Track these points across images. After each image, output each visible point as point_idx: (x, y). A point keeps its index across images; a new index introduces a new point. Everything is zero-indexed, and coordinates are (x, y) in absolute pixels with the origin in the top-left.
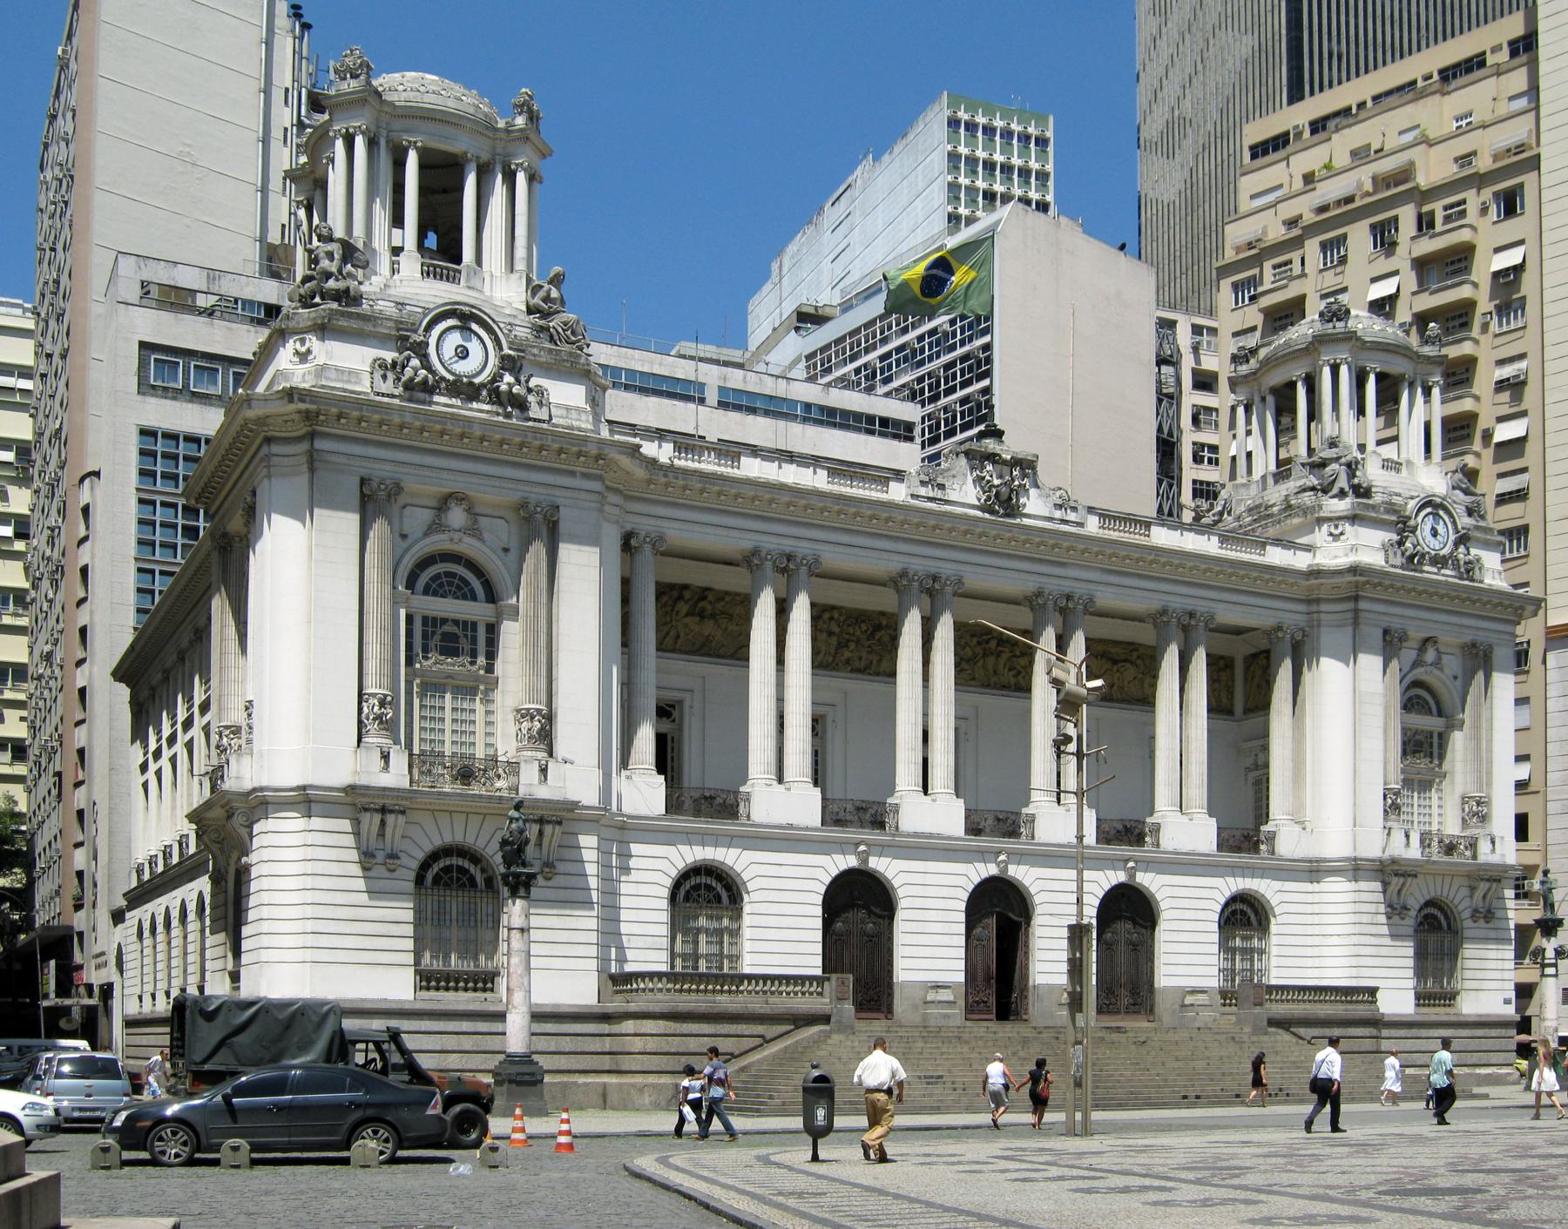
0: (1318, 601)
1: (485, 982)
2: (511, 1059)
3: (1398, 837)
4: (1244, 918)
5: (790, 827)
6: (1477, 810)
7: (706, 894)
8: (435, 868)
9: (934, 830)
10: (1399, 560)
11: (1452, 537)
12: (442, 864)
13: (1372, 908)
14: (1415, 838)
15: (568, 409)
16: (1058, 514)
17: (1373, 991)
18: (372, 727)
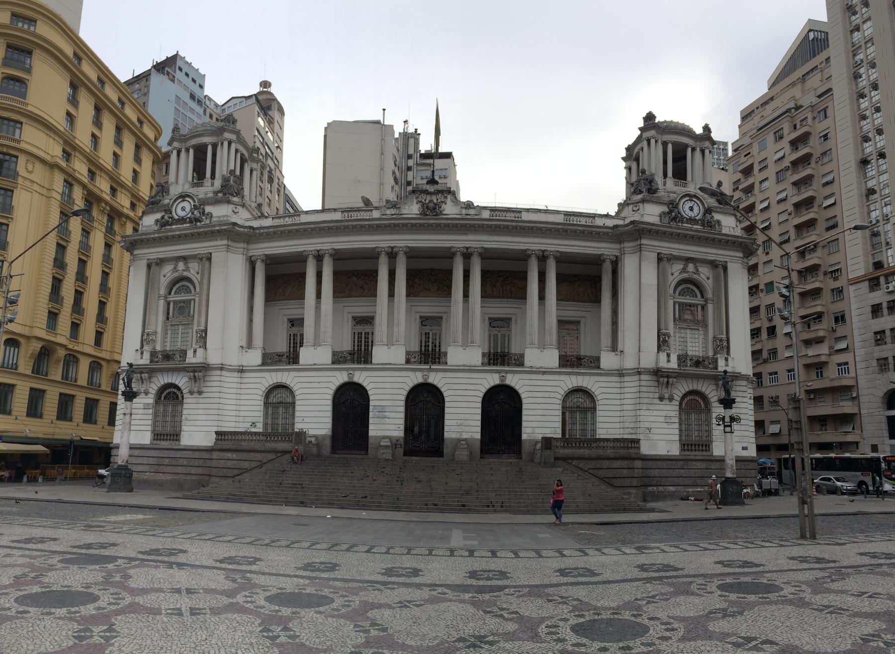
3: (663, 356)
8: (165, 393)
12: (167, 391)
14: (674, 358)
17: (638, 441)
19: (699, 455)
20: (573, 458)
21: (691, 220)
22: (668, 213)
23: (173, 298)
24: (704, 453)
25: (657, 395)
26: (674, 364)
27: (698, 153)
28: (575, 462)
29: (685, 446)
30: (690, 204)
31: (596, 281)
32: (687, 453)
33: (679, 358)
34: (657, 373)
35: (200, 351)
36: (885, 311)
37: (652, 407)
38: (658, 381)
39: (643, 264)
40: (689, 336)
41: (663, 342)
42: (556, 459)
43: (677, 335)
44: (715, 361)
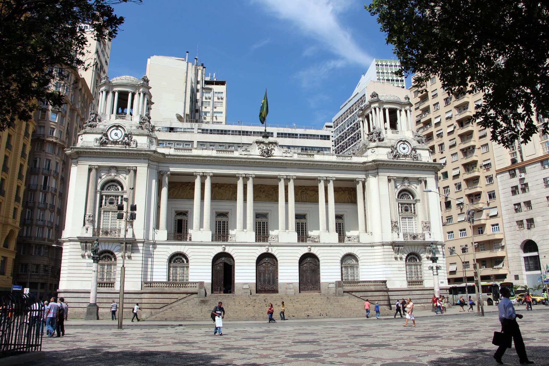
0: (368, 170)
1: (112, 284)
2: (91, 305)
3: (395, 234)
4: (349, 260)
5: (202, 242)
6: (427, 226)
7: (177, 259)
9: (243, 241)
10: (392, 157)
11: (410, 149)
13: (390, 256)
14: (401, 235)
15: (142, 144)
16: (284, 155)
18: (87, 222)
19: (417, 287)
20: (352, 292)
21: (405, 156)
22: (392, 152)
23: (105, 192)
24: (420, 286)
25: (393, 256)
26: (401, 239)
27: (403, 112)
28: (353, 293)
29: (410, 283)
30: (403, 146)
31: (354, 191)
32: (410, 286)
33: (404, 235)
34: (394, 244)
35: (130, 231)
36: (520, 191)
37: (391, 263)
38: (393, 249)
39: (380, 183)
40: (407, 221)
41: (395, 226)
42: (344, 292)
43: (401, 222)
44: (423, 235)
